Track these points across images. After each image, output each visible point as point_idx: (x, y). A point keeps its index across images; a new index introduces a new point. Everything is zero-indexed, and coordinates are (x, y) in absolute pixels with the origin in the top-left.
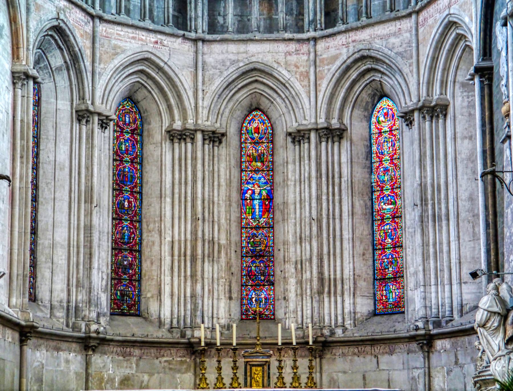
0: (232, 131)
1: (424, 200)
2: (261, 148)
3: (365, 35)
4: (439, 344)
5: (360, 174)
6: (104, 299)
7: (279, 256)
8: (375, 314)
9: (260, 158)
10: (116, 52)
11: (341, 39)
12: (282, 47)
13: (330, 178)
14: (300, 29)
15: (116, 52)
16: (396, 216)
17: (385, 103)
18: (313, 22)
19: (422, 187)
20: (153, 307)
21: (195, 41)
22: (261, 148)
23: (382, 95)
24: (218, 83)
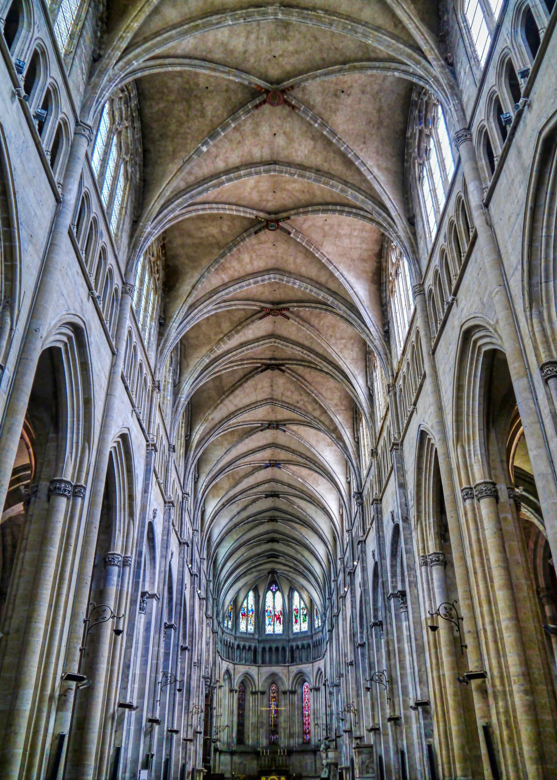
0: (267, 690)
1: (314, 713)
2: (275, 695)
3: (300, 666)
4: (318, 753)
5: (300, 703)
6: (235, 740)
7: (279, 725)
8: (303, 743)
9: (275, 697)
10: (239, 672)
11: (295, 667)
12: (280, 668)
13: (292, 704)
14: (285, 663)
15: (239, 672)
16: (309, 716)
17: (306, 684)
18: (288, 661)
19: (314, 710)
20: (247, 742)
21: (259, 666)
22: (275, 695)
23: (305, 681)
24: (264, 677)
